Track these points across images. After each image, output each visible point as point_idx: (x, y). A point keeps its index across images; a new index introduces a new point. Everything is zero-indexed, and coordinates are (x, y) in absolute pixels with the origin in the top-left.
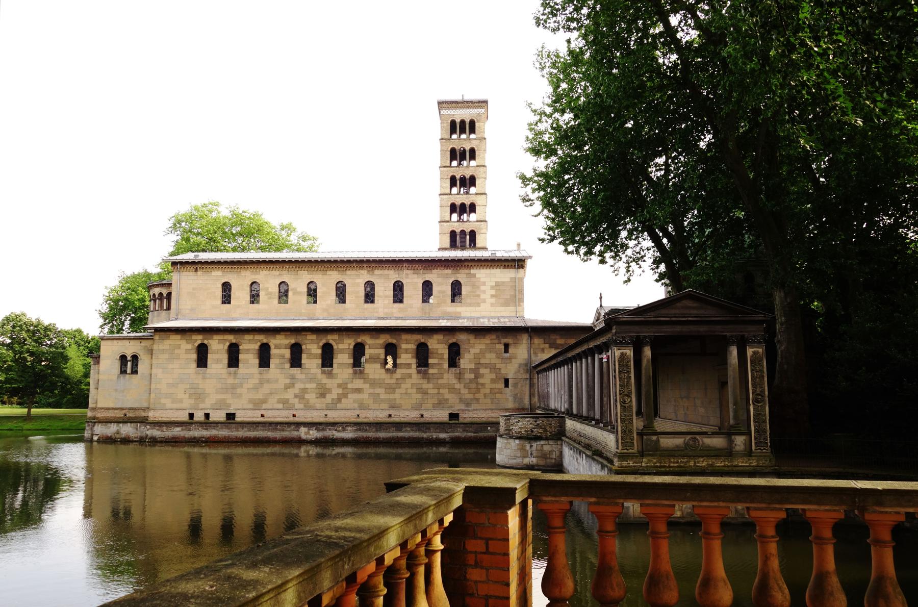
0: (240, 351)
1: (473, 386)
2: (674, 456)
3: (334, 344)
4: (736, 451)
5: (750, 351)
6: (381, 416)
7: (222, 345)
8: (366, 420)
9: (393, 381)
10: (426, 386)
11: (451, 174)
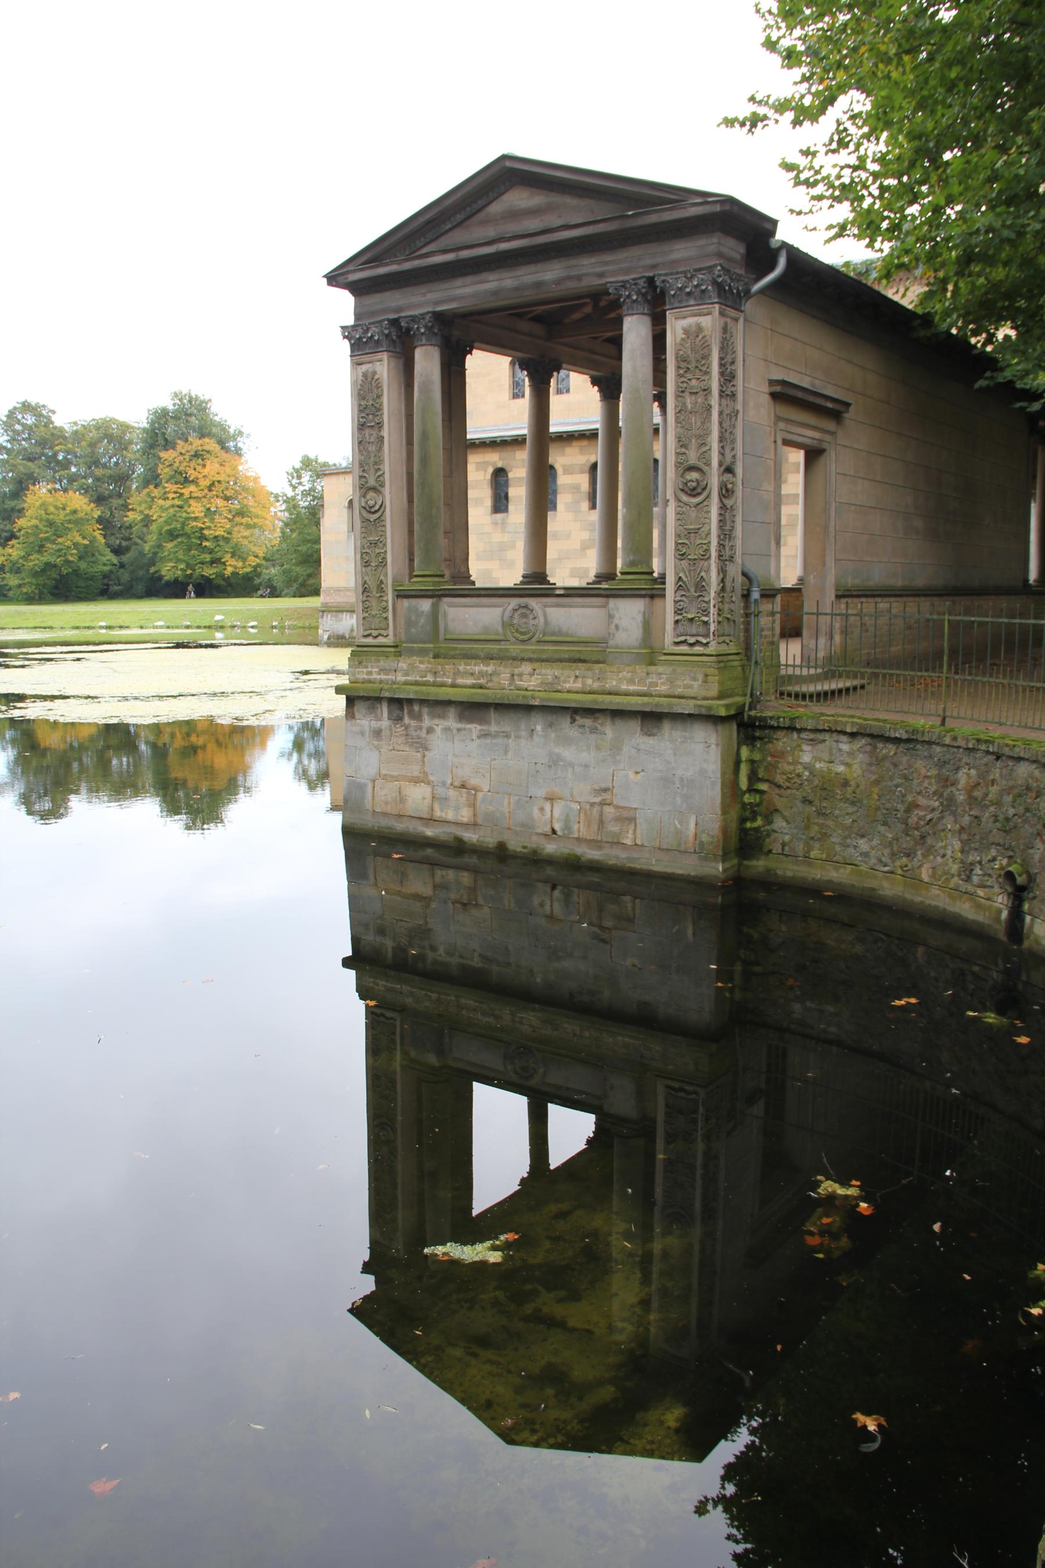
0: (510, 482)
4: (617, 647)
5: (676, 327)
7: (482, 473)
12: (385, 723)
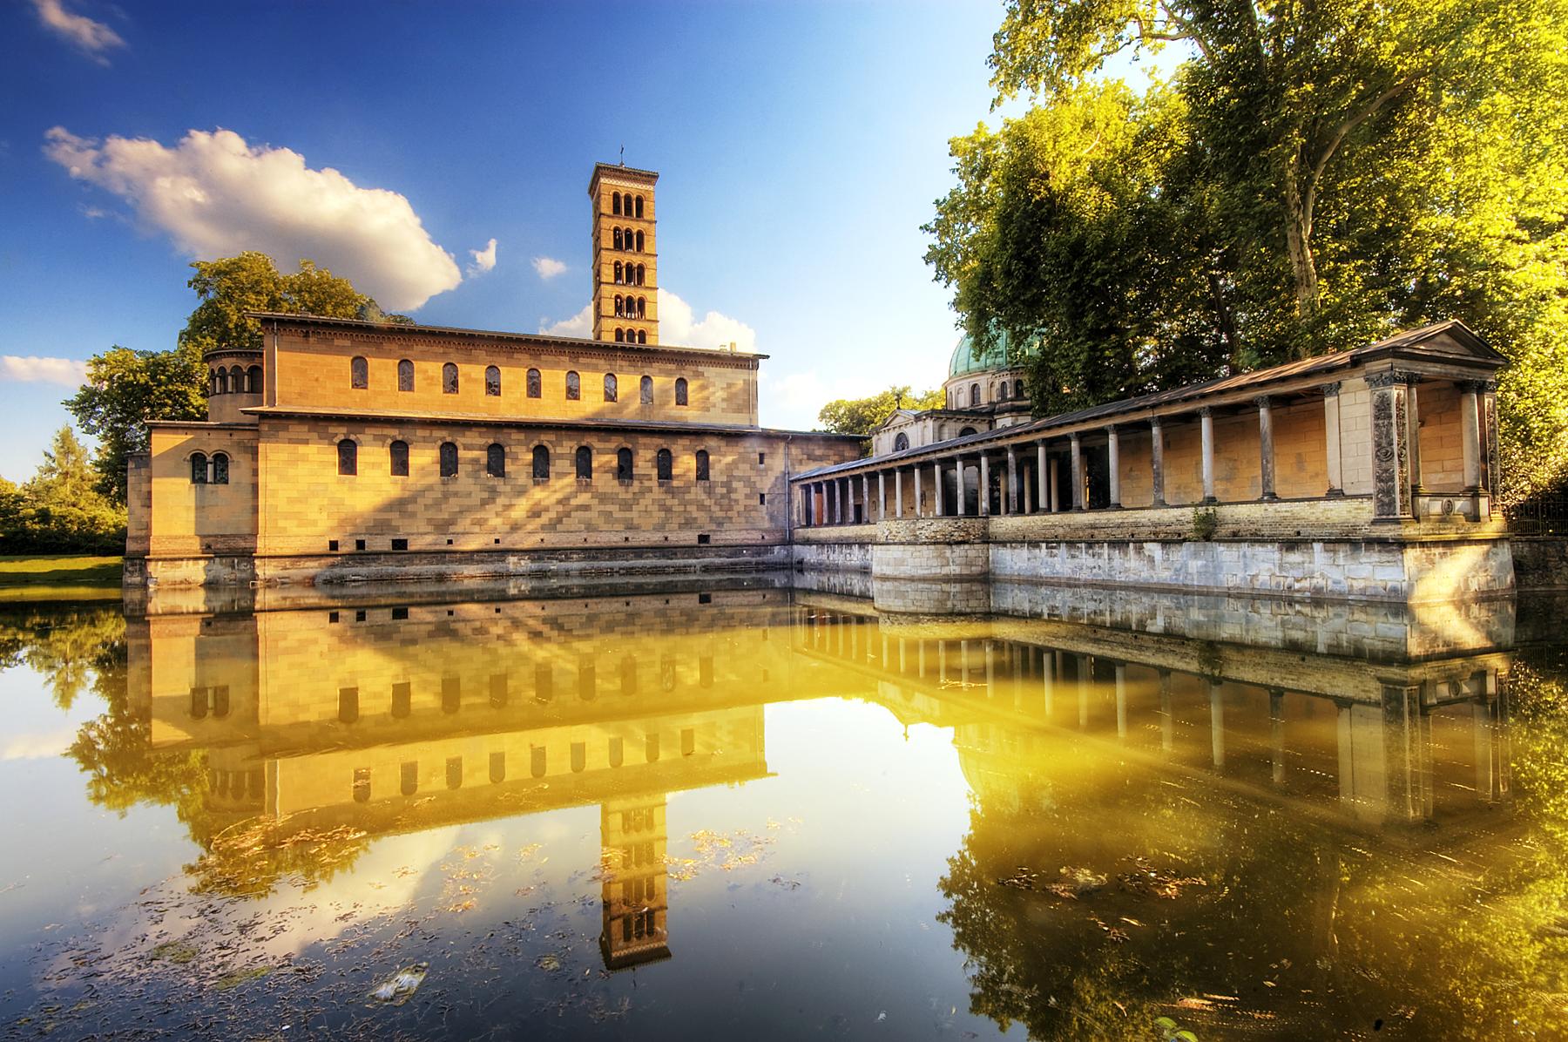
1: (725, 502)
3: (549, 446)
6: (615, 539)
9: (630, 496)
10: (672, 502)
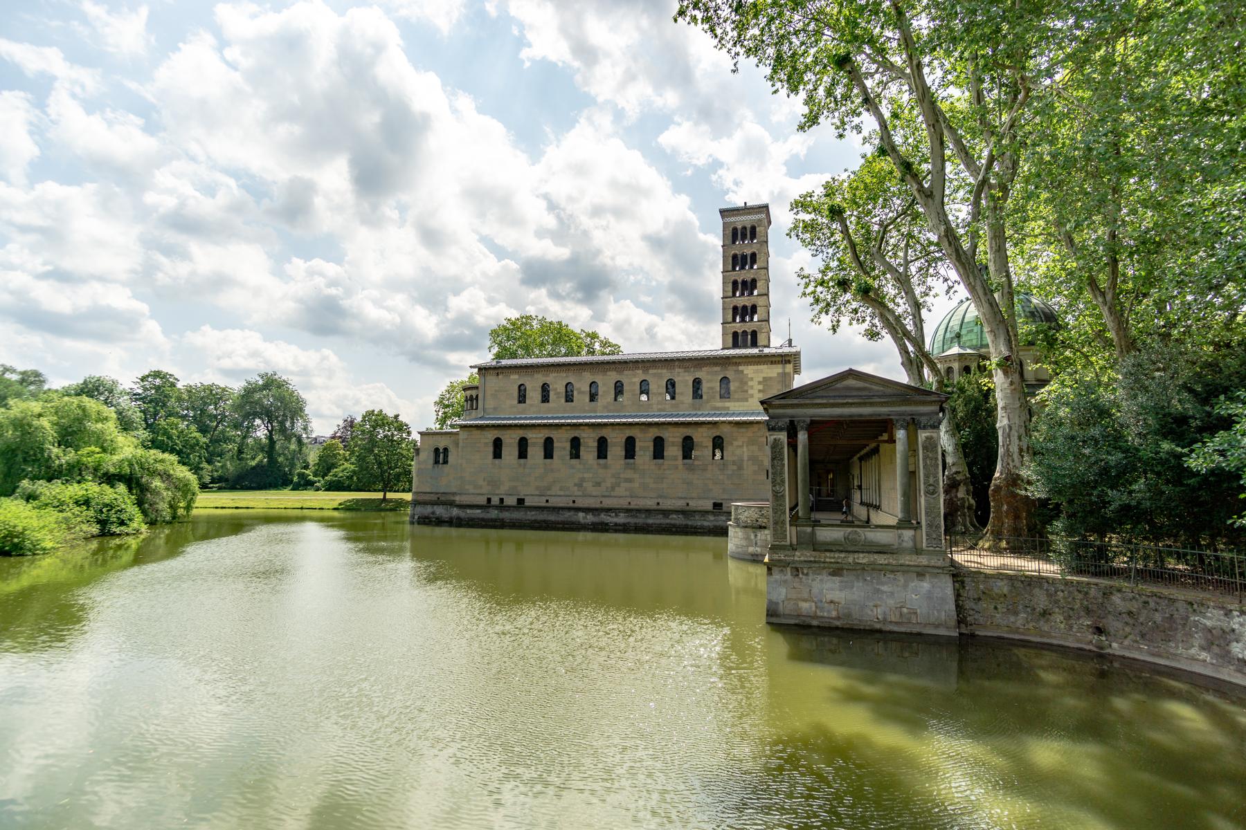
2: (831, 551)
8: (637, 507)
11: (733, 278)
12: (789, 576)
